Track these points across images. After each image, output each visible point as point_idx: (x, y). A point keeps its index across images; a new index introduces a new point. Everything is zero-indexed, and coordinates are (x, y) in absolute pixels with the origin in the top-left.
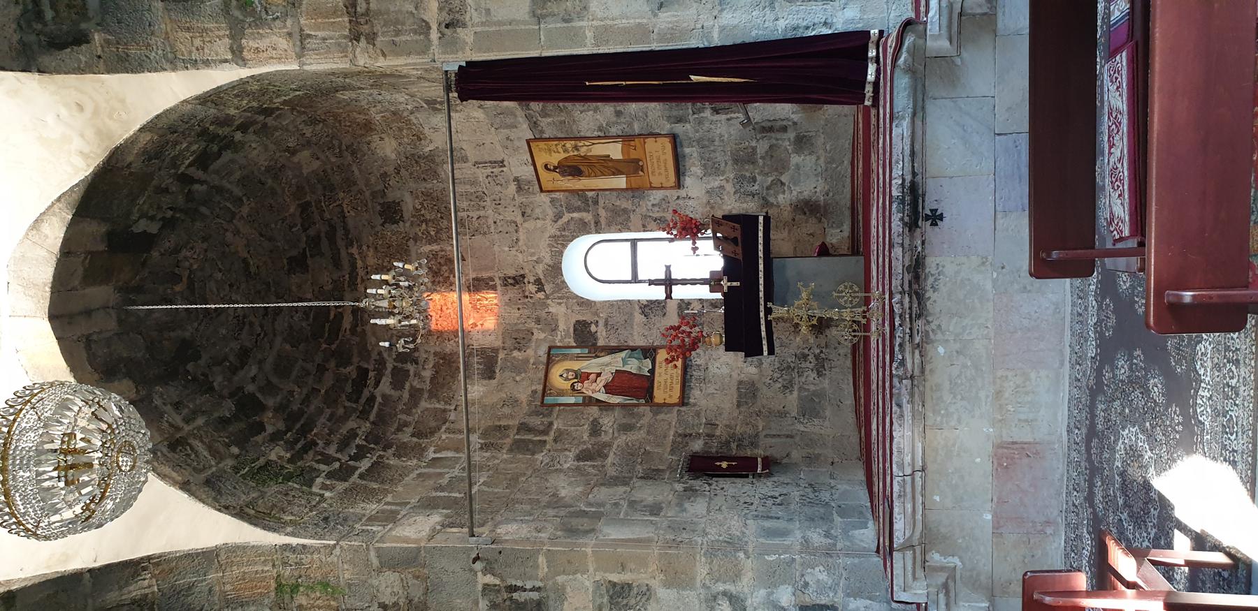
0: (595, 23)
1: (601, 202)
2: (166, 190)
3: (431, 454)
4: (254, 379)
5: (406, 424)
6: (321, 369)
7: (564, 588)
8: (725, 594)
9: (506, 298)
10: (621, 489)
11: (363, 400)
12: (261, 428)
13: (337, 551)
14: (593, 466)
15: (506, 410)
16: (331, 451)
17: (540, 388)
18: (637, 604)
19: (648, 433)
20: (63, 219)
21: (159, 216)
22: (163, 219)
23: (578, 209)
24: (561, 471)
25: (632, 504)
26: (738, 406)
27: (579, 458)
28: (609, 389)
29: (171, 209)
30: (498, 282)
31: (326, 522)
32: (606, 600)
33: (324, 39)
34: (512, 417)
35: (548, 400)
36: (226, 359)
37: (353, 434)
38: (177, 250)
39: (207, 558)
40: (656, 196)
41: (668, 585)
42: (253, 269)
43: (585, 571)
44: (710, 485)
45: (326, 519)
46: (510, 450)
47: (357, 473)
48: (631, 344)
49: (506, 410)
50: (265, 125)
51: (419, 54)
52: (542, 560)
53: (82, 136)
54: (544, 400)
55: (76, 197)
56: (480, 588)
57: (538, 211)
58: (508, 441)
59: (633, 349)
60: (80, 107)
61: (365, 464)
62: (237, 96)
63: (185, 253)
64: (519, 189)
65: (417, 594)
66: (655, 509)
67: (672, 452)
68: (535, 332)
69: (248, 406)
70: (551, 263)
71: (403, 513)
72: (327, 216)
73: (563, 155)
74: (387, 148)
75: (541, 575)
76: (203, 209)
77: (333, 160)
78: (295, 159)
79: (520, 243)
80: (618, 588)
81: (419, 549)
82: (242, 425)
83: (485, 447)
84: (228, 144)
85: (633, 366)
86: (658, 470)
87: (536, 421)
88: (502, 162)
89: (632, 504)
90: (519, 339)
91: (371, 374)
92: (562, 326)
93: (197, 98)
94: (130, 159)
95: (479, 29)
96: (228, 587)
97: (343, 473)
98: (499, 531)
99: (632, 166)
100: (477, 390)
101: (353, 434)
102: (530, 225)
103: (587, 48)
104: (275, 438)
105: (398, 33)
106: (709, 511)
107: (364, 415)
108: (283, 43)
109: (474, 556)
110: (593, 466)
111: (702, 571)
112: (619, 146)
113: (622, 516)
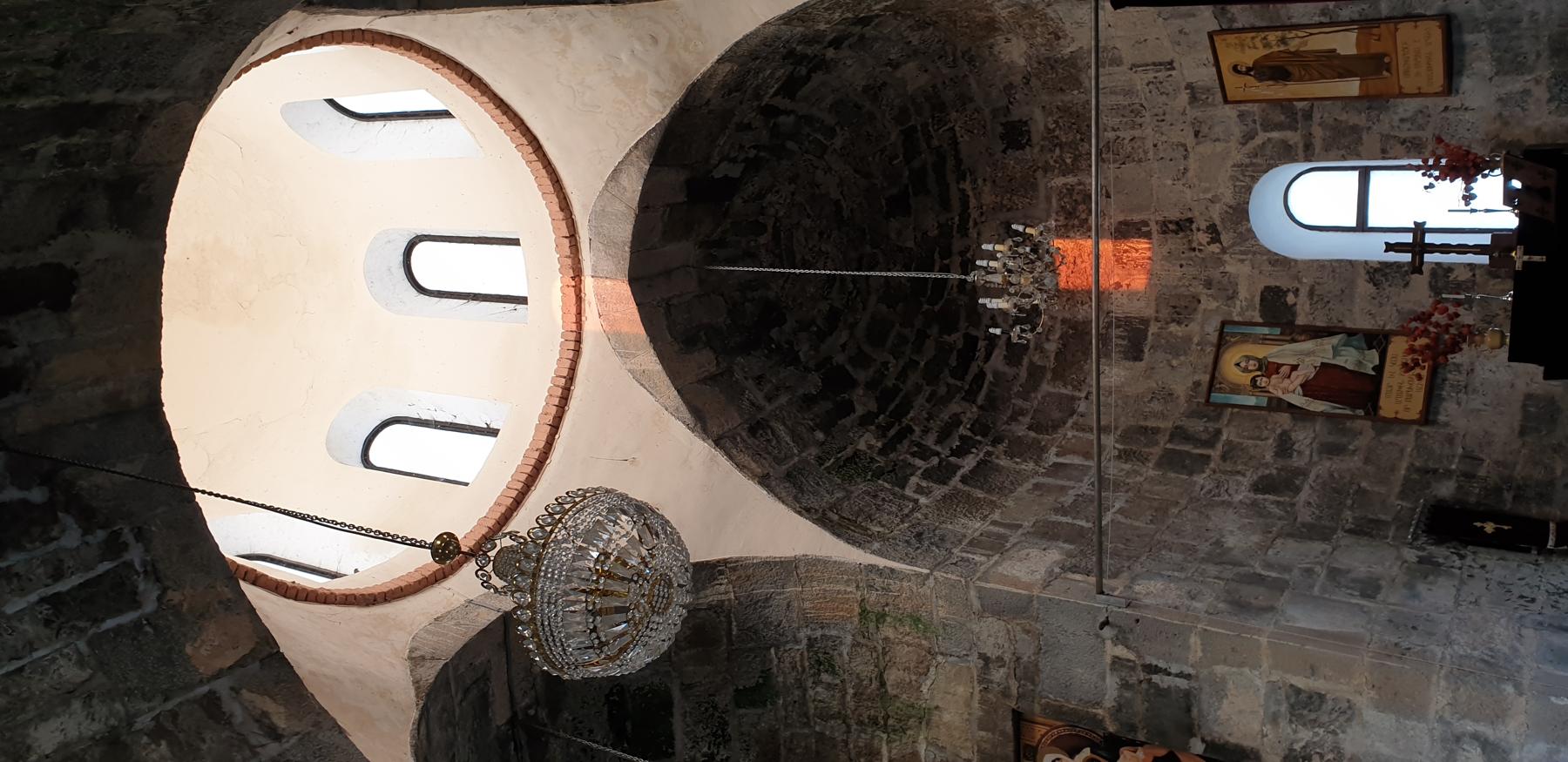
1: (1317, 116)
2: (749, 127)
3: (1052, 458)
4: (843, 347)
5: (1022, 412)
6: (922, 336)
7: (1224, 680)
8: (1475, 737)
9: (1165, 250)
10: (1318, 547)
11: (969, 378)
12: (848, 408)
13: (931, 579)
14: (1278, 503)
15: (1156, 406)
16: (930, 441)
17: (1207, 378)
18: (1331, 723)
19: (1367, 461)
20: (640, 169)
21: (742, 157)
22: (746, 160)
23: (1279, 127)
25: (1334, 573)
26: (1523, 432)
27: (1256, 488)
28: (1308, 389)
29: (754, 147)
30: (1154, 228)
31: (920, 540)
32: (1284, 708)
34: (1164, 416)
35: (1217, 397)
37: (956, 421)
39: (786, 569)
40: (1408, 107)
41: (1381, 706)
42: (846, 214)
43: (1255, 666)
44: (1462, 557)
45: (919, 535)
46: (1159, 465)
47: (959, 473)
48: (1348, 325)
49: (1156, 406)
50: (862, 37)
52: (1194, 640)
53: (657, 73)
54: (1210, 398)
55: (653, 143)
56: (1108, 660)
57: (1218, 130)
58: (1157, 451)
59: (1351, 333)
60: (655, 40)
61: (969, 463)
62: (826, 9)
64: (1194, 99)
65: (1027, 653)
66: (1370, 588)
67: (1403, 495)
68: (1203, 299)
69: (837, 381)
70: (1233, 203)
71: (1013, 540)
72: (935, 143)
73: (1267, 52)
74: (1014, 51)
75: (1192, 659)
76: (790, 145)
77: (945, 71)
78: (899, 74)
79: (1190, 174)
80: (1303, 697)
81: (1030, 599)
82: (829, 405)
83: (1124, 456)
84: (820, 64)
85: (1349, 359)
86: (1378, 521)
87: (1198, 426)
88: (1171, 63)
89: (1334, 573)
90: (1180, 308)
92: (1243, 293)
93: (781, 18)
94: (709, 94)
96: (807, 605)
97: (941, 474)
98: (1137, 588)
99: (1371, 64)
100: (1116, 374)
101: (956, 421)
102: (1206, 148)
104: (866, 421)
106: (1457, 603)
107: (970, 397)
109: (1102, 619)
110: (1278, 503)
111: (1439, 697)
112: (1353, 36)
113: (1316, 591)
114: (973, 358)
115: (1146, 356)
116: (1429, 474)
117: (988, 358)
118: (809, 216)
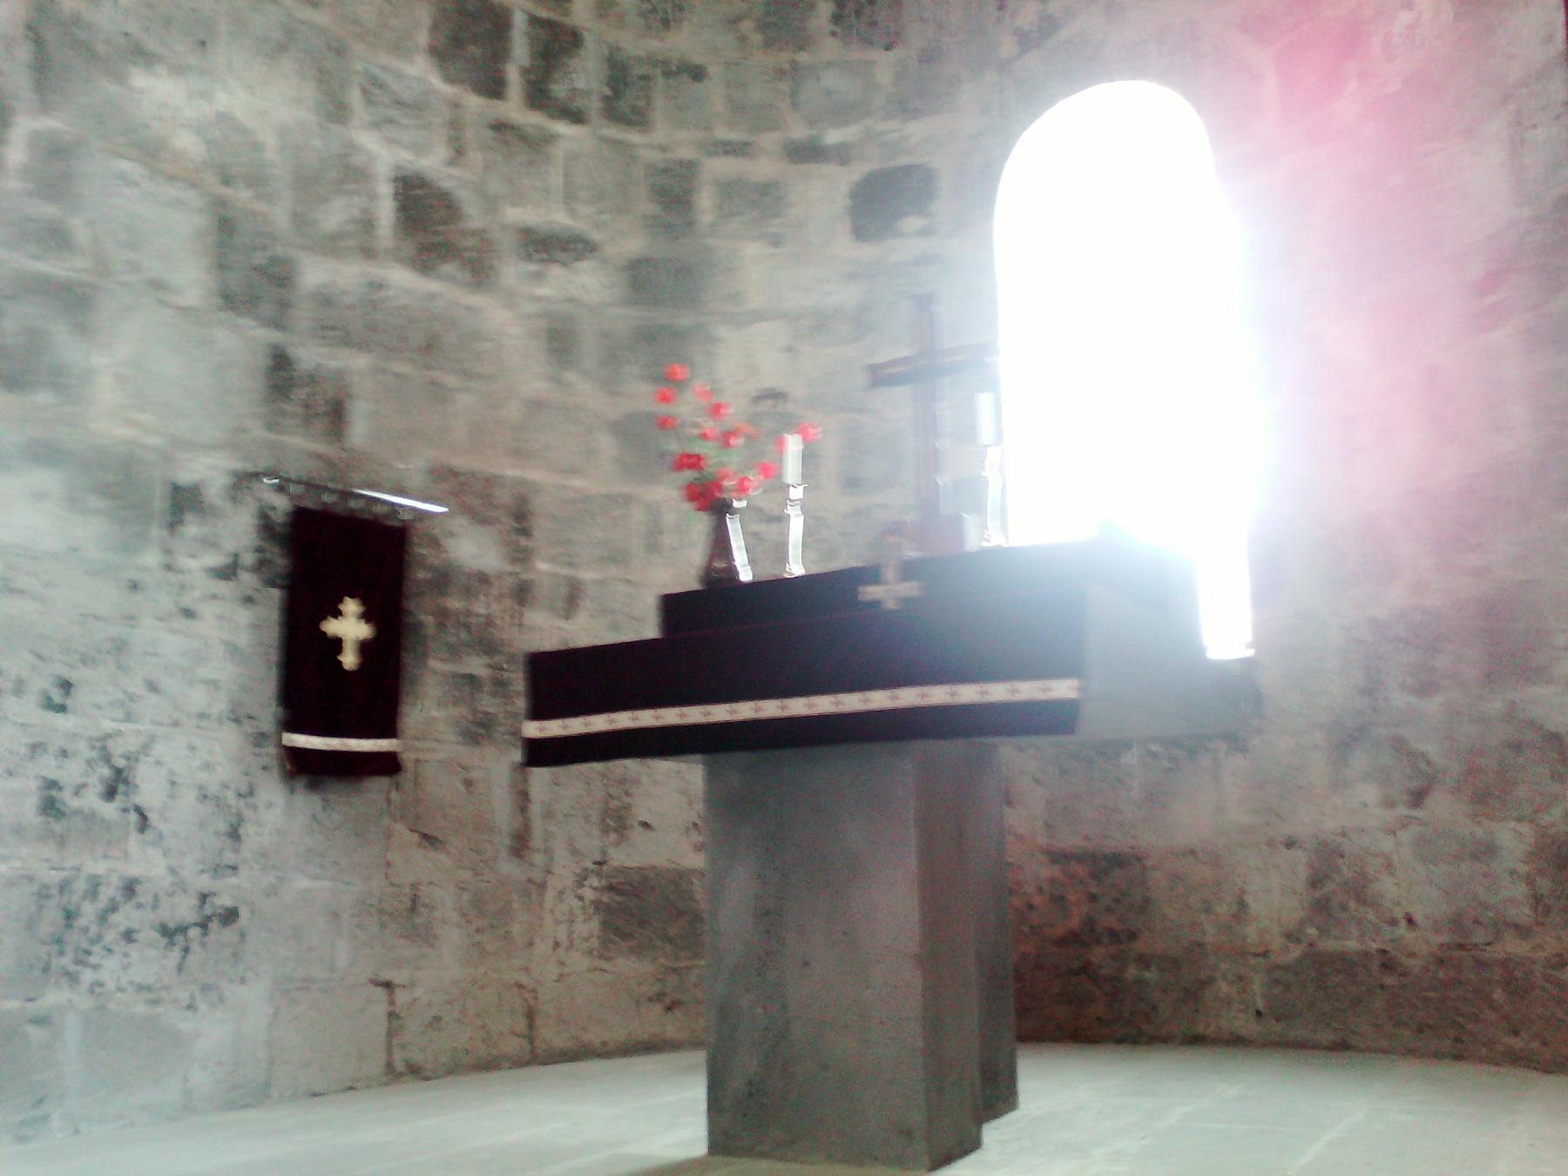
10: (192, 280)
19: (537, 405)
24: (337, 111)
87: (584, 76)
110: (367, 224)
116: (520, 521)
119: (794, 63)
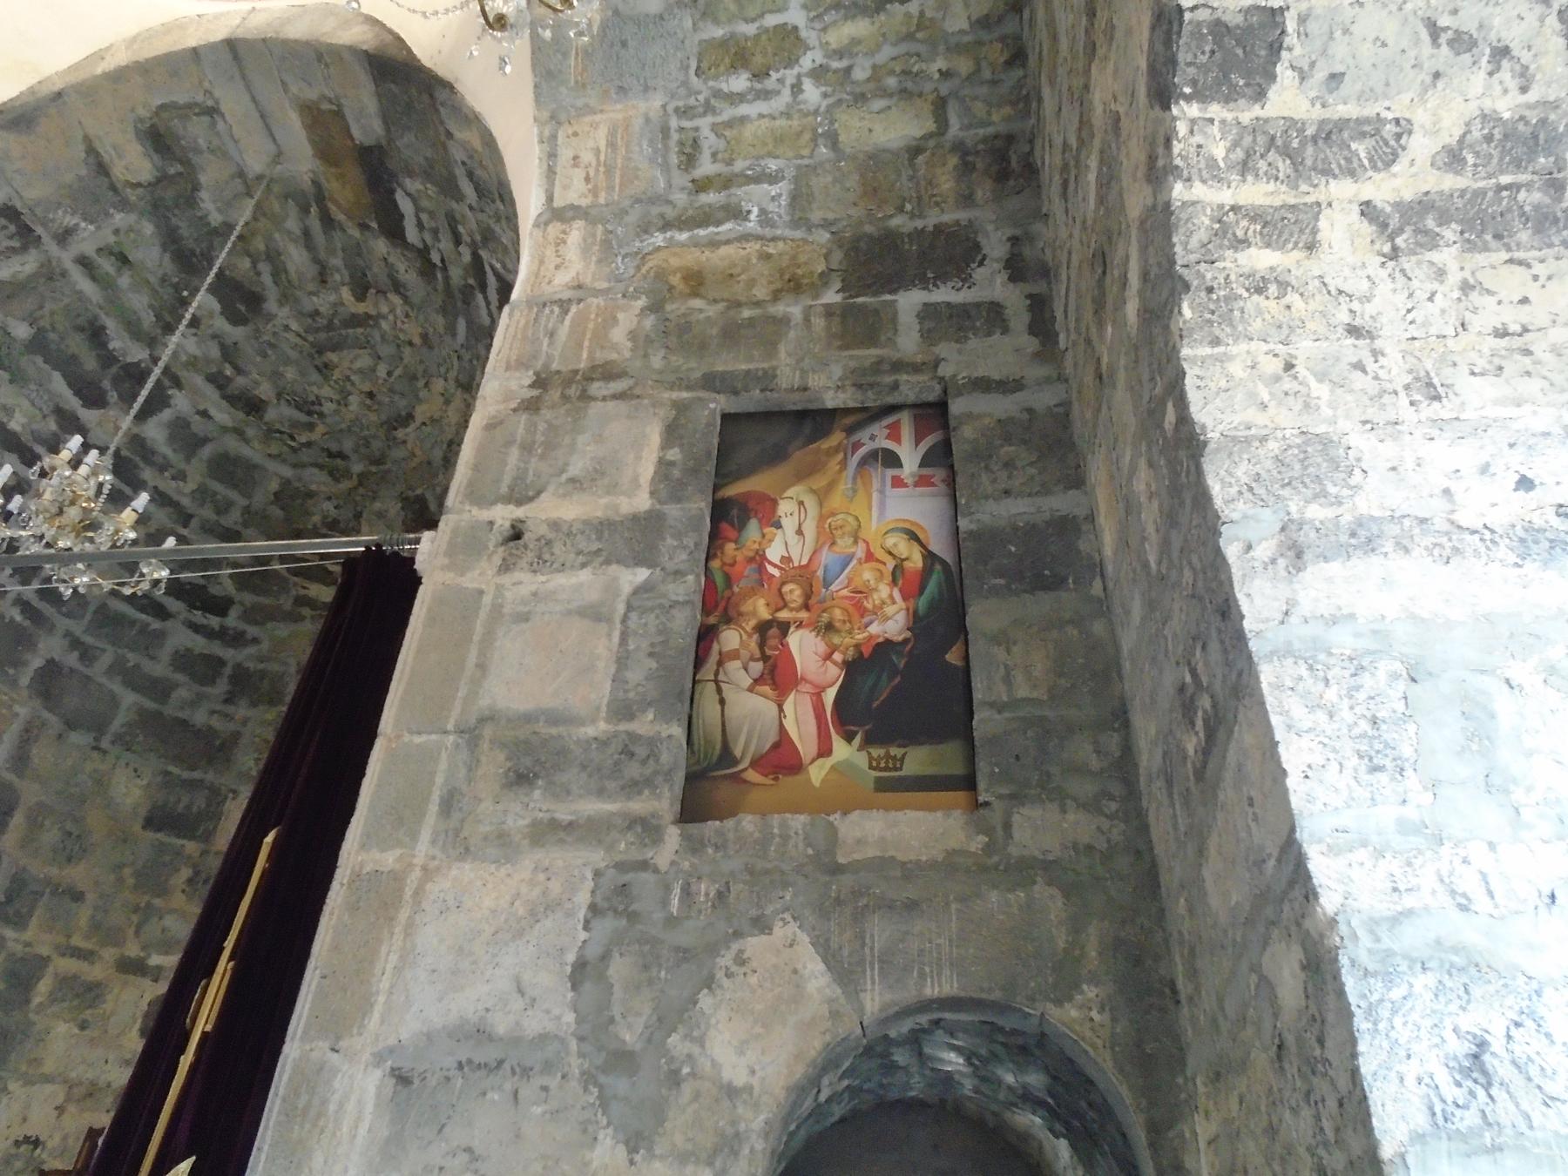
0: (417, 874)
4: (204, 414)
33: (552, 335)
36: (239, 371)
38: (398, 287)
42: (400, 434)
51: (470, 484)
55: (392, 52)
63: (396, 300)
76: (461, 325)
91: (214, 622)
95: (487, 600)
103: (357, 852)
105: (527, 448)
108: (563, 278)
114: (192, 606)
115: (150, 835)
117: (196, 628)
118: (389, 374)
119: (149, 905)
